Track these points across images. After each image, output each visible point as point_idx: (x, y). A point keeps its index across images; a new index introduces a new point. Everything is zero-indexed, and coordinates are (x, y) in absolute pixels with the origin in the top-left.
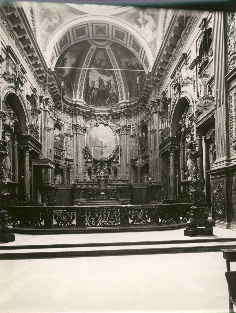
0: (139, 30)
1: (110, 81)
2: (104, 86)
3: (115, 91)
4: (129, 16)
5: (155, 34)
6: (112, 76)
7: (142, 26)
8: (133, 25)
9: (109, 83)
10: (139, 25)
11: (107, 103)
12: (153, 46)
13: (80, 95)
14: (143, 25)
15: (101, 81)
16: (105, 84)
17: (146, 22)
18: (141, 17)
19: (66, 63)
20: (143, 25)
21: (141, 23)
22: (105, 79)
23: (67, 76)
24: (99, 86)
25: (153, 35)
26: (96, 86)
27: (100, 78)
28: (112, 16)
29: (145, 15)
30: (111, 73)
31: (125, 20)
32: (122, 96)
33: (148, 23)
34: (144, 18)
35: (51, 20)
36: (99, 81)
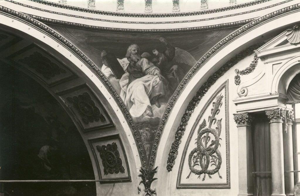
0: (113, 80)
4: (94, 41)
5: (158, 111)
7: (124, 76)
8: (101, 66)
10: (118, 72)
12: (145, 133)
14: (127, 74)
17: (136, 72)
18: (129, 58)
20: (127, 74)
21: (125, 68)
25: (149, 108)
28: (40, 23)
29: (141, 58)
31: (78, 45)
33: (145, 78)
34: (135, 62)
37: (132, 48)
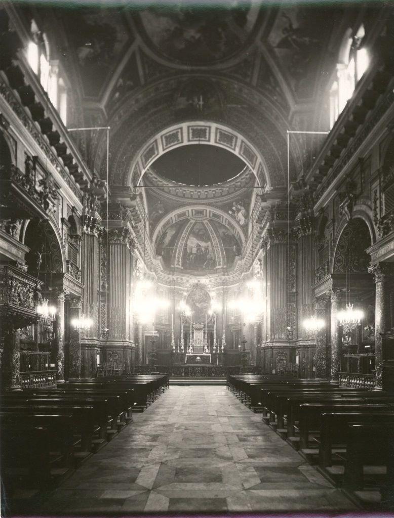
1: (208, 246)
2: (202, 251)
3: (212, 256)
6: (209, 243)
9: (207, 249)
11: (204, 267)
13: (178, 261)
15: (199, 246)
16: (203, 249)
17: (239, 211)
19: (166, 236)
22: (203, 244)
23: (167, 246)
24: (197, 251)
26: (194, 251)
27: (198, 244)
30: (208, 239)
32: (219, 262)
35: (158, 212)
36: (197, 246)
37: (234, 203)
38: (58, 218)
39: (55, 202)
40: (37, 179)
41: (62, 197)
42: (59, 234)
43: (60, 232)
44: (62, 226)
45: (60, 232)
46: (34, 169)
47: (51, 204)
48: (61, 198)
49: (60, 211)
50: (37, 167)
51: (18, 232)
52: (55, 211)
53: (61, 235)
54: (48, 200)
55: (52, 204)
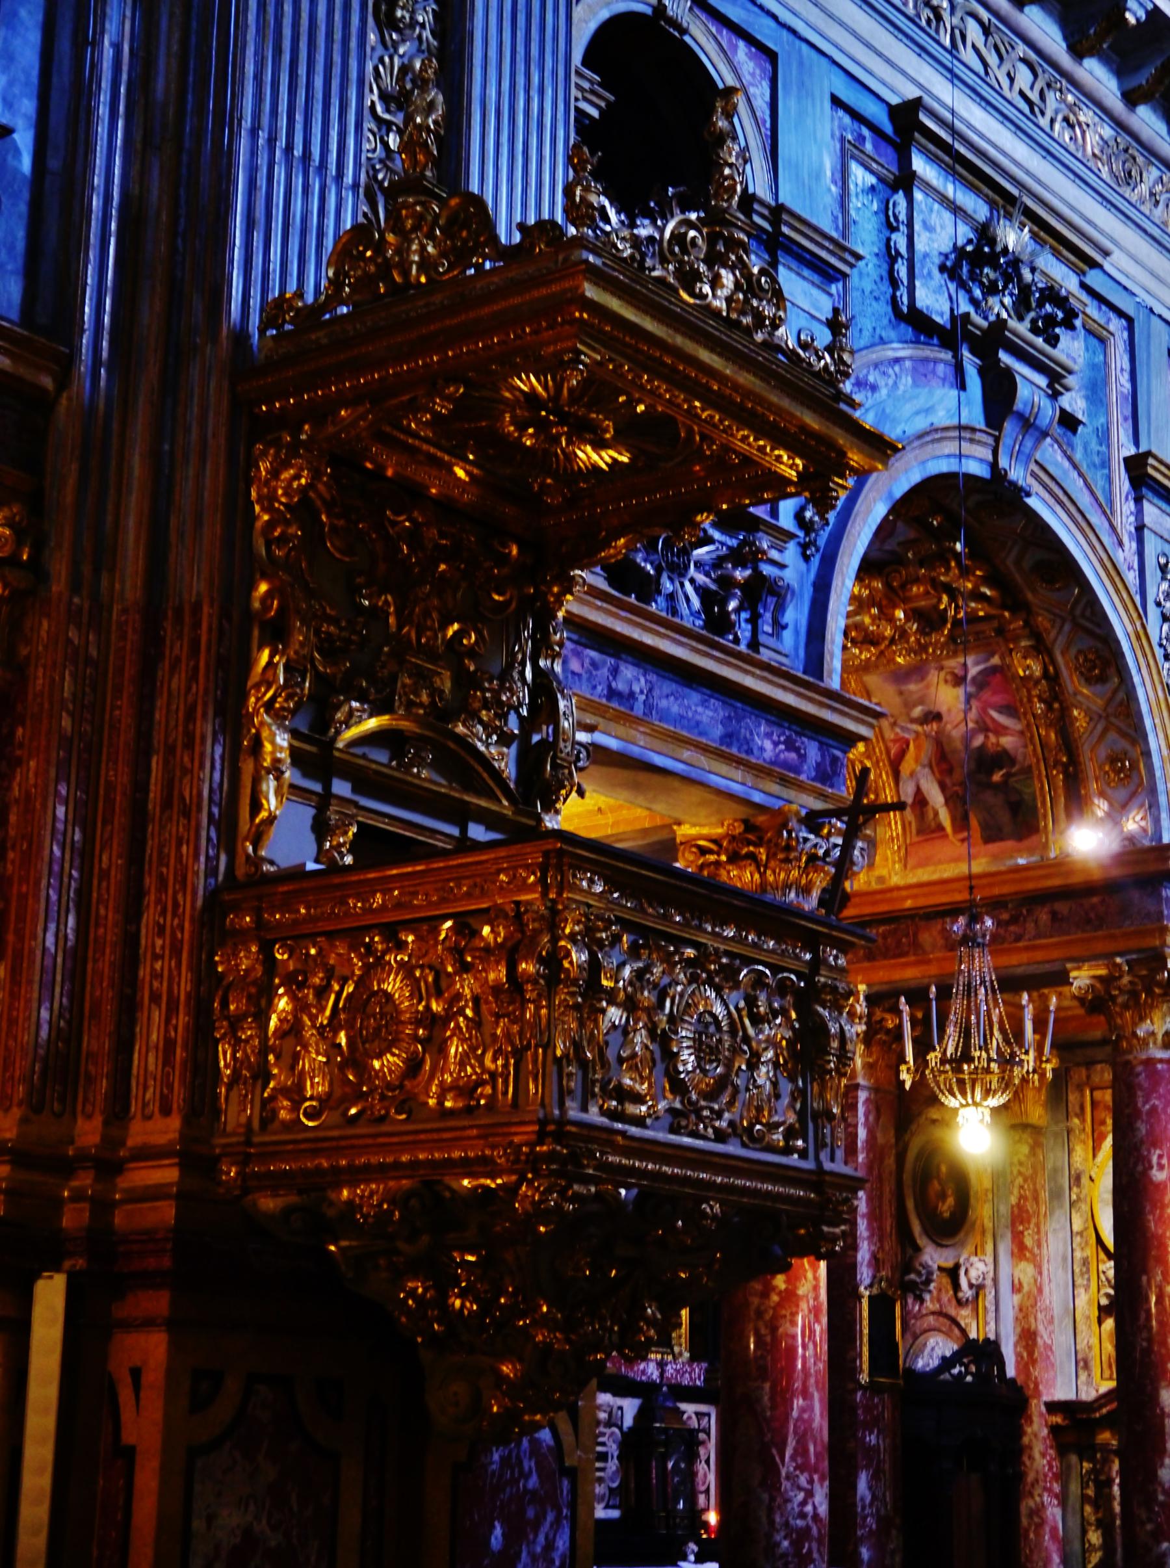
38: (1106, 463)
39: (1071, 348)
40: (920, 245)
41: (1121, 314)
42: (1113, 571)
43: (1126, 556)
44: (1139, 513)
45: (1126, 556)
46: (905, 181)
47: (1030, 386)
48: (1116, 325)
49: (1118, 412)
50: (919, 164)
51: (796, 614)
52: (1069, 422)
53: (1132, 578)
54: (1005, 358)
55: (1042, 381)
